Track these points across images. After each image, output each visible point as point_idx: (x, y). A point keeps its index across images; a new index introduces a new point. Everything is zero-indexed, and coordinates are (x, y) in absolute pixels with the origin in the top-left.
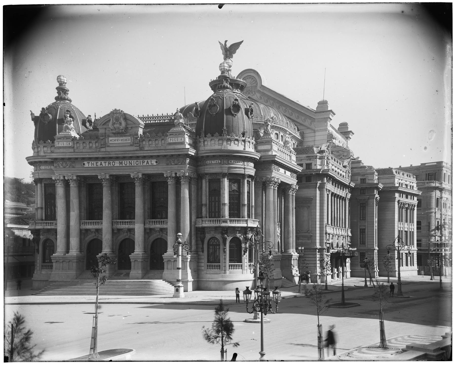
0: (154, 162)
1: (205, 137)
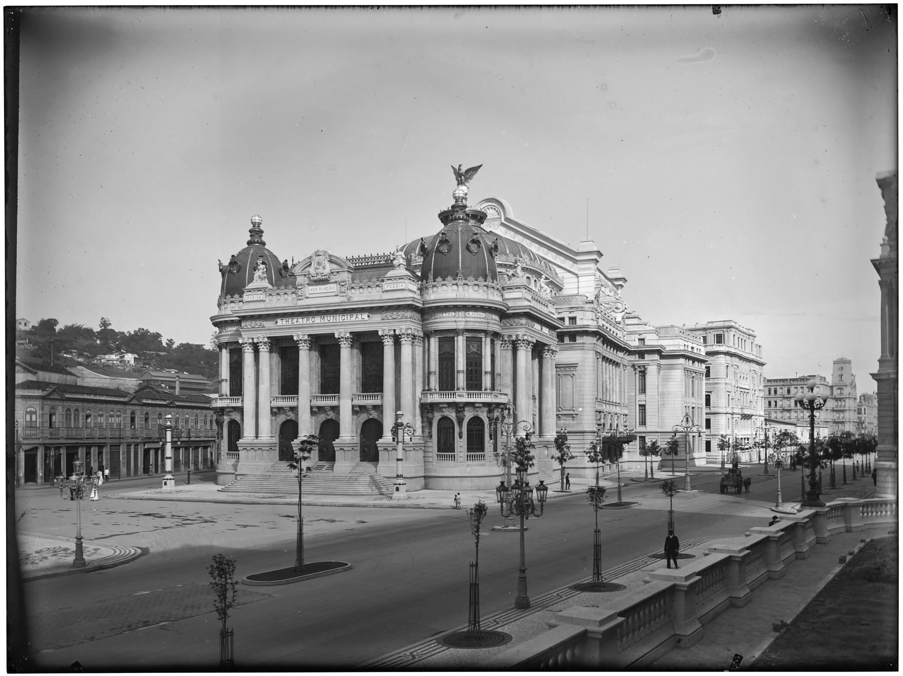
0: (365, 316)
1: (434, 281)
